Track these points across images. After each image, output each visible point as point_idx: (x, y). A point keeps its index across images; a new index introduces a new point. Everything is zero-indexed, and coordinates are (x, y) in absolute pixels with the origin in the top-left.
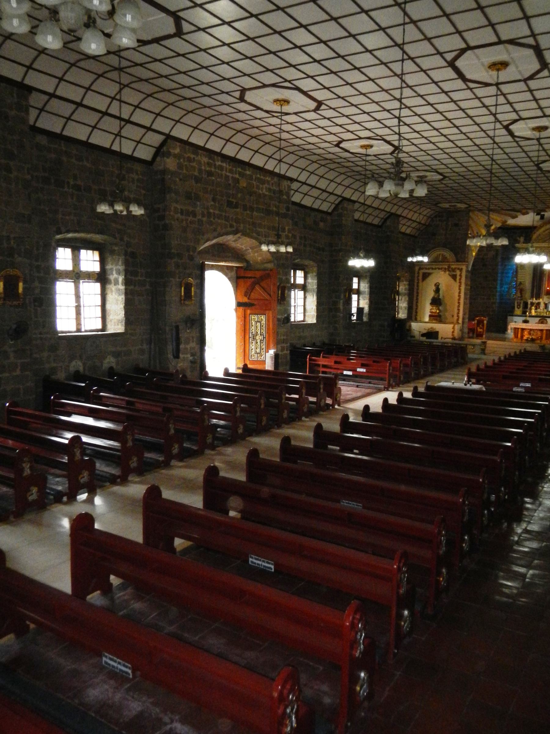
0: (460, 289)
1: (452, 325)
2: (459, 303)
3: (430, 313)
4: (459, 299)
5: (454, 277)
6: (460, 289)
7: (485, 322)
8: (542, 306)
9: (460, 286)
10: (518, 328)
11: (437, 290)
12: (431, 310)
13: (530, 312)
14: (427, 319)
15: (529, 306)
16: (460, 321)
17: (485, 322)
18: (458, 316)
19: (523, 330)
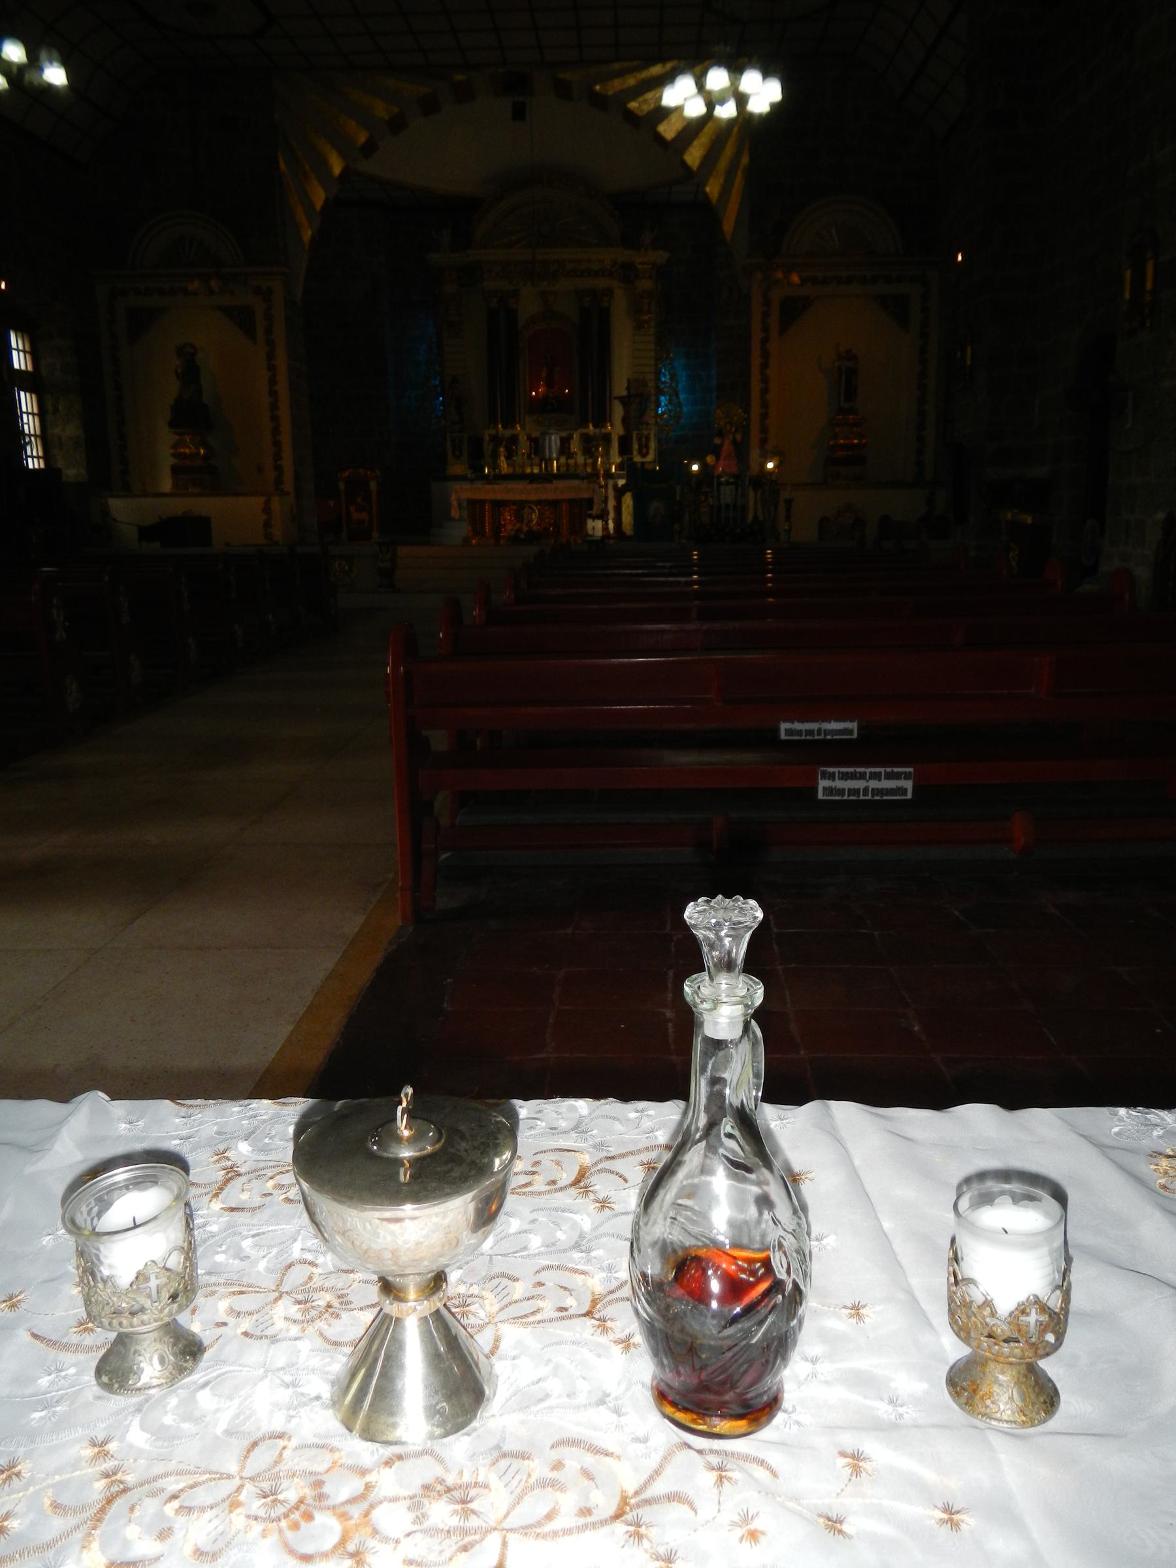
0: (271, 368)
1: (263, 499)
2: (275, 418)
3: (172, 461)
4: (274, 406)
5: (243, 319)
6: (271, 368)
7: (373, 485)
8: (524, 447)
9: (271, 356)
10: (482, 502)
11: (190, 373)
12: (175, 446)
13: (495, 466)
14: (166, 485)
15: (488, 448)
16: (288, 484)
17: (373, 485)
18: (278, 469)
19: (498, 505)
